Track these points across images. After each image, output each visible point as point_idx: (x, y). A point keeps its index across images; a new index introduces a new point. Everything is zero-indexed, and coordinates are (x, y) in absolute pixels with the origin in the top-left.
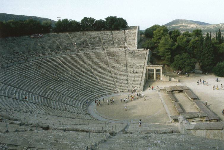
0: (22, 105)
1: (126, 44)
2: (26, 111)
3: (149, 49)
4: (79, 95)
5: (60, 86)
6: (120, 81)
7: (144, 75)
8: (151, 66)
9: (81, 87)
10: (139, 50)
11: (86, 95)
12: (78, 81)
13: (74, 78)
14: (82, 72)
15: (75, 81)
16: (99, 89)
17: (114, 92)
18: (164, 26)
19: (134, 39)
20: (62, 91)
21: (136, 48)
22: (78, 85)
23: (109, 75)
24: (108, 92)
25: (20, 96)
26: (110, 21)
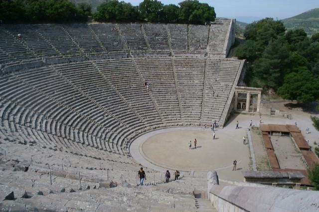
0: (21, 133)
1: (208, 48)
2: (23, 142)
3: (244, 60)
4: (119, 124)
5: (92, 108)
6: (189, 107)
7: (229, 102)
8: (243, 87)
9: (126, 111)
10: (227, 60)
11: (131, 126)
12: (121, 102)
13: (117, 97)
14: (130, 88)
15: (117, 101)
16: (153, 117)
17: (176, 124)
18: (279, 22)
19: (223, 41)
20: (94, 115)
21: (225, 56)
22: (120, 108)
23: (173, 97)
24: (167, 123)
25: (24, 118)
26: (187, 8)
